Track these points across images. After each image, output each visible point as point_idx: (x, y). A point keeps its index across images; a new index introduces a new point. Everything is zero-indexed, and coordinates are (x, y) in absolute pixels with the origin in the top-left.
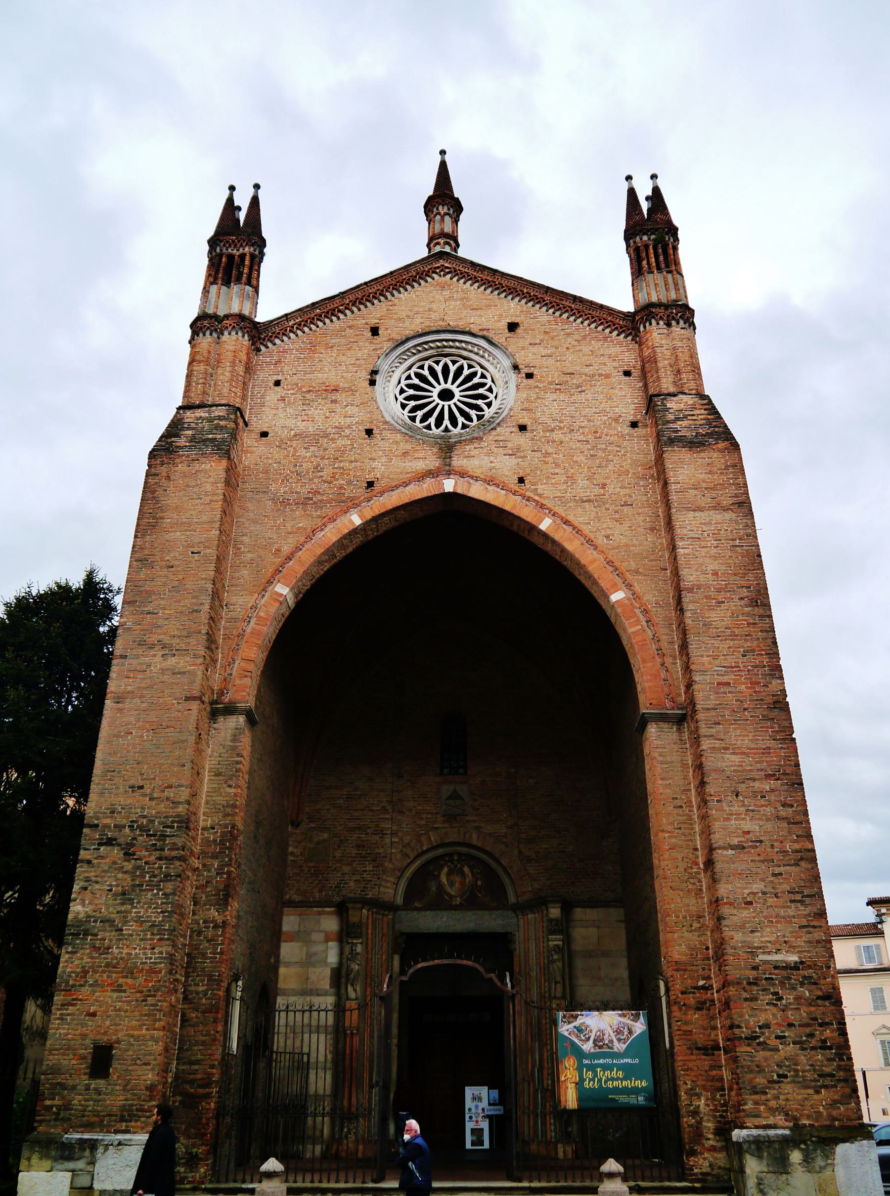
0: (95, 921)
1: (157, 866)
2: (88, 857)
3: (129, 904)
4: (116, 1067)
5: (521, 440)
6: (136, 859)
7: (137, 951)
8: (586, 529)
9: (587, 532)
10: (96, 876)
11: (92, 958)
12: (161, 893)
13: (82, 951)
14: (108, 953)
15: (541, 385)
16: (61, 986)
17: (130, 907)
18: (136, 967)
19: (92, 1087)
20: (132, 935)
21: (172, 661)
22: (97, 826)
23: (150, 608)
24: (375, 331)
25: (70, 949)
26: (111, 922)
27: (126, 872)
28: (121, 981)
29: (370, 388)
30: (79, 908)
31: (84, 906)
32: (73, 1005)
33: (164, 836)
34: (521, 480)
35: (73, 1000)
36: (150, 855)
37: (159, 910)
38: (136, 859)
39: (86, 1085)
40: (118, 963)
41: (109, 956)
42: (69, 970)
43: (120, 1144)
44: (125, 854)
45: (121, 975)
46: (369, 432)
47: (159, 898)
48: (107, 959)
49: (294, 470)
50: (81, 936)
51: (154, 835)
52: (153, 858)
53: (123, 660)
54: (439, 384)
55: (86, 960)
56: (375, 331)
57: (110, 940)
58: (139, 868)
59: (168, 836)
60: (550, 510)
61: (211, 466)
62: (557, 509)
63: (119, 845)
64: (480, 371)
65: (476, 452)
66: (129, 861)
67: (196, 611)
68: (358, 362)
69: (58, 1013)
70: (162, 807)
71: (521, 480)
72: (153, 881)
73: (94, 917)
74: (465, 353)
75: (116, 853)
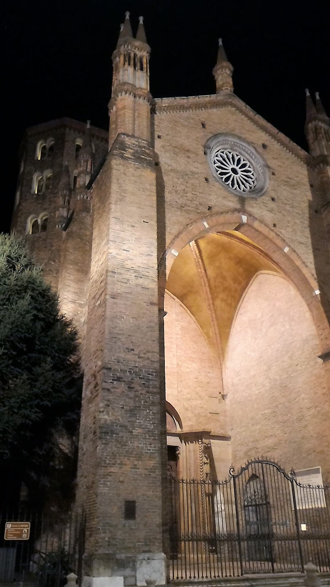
0: (117, 426)
1: (147, 396)
2: (108, 387)
3: (135, 417)
4: (138, 513)
5: (272, 205)
6: (135, 391)
7: (142, 445)
8: (301, 256)
9: (303, 258)
10: (114, 399)
11: (117, 447)
12: (151, 412)
13: (111, 444)
14: (126, 445)
15: (279, 180)
16: (102, 464)
17: (135, 419)
18: (143, 455)
19: (127, 525)
20: (137, 435)
21: (140, 281)
22: (110, 369)
23: (125, 247)
24: (203, 125)
25: (104, 442)
26: (125, 427)
27: (130, 398)
28: (136, 462)
29: (204, 156)
30: (106, 417)
31: (109, 416)
32: (110, 476)
33: (148, 380)
34: (275, 225)
35: (110, 472)
36: (142, 390)
37: (151, 422)
38: (135, 391)
39: (124, 524)
40: (132, 451)
41: (127, 447)
42: (105, 454)
43: (149, 559)
44: (129, 387)
45: (135, 459)
46: (206, 180)
47: (151, 415)
48: (126, 448)
49: (173, 189)
50: (110, 434)
51: (144, 379)
52: (144, 392)
53: (113, 274)
54: (234, 164)
55: (115, 449)
56: (203, 125)
57: (126, 438)
58: (137, 396)
59: (150, 380)
60: (287, 244)
61: (148, 174)
62: (291, 245)
63: (125, 382)
64: (248, 164)
65: (255, 205)
66: (130, 391)
67: (150, 255)
68: (197, 139)
69: (102, 480)
70: (146, 362)
71: (275, 225)
72: (146, 405)
73: (116, 423)
74: (243, 152)
75: (123, 387)
